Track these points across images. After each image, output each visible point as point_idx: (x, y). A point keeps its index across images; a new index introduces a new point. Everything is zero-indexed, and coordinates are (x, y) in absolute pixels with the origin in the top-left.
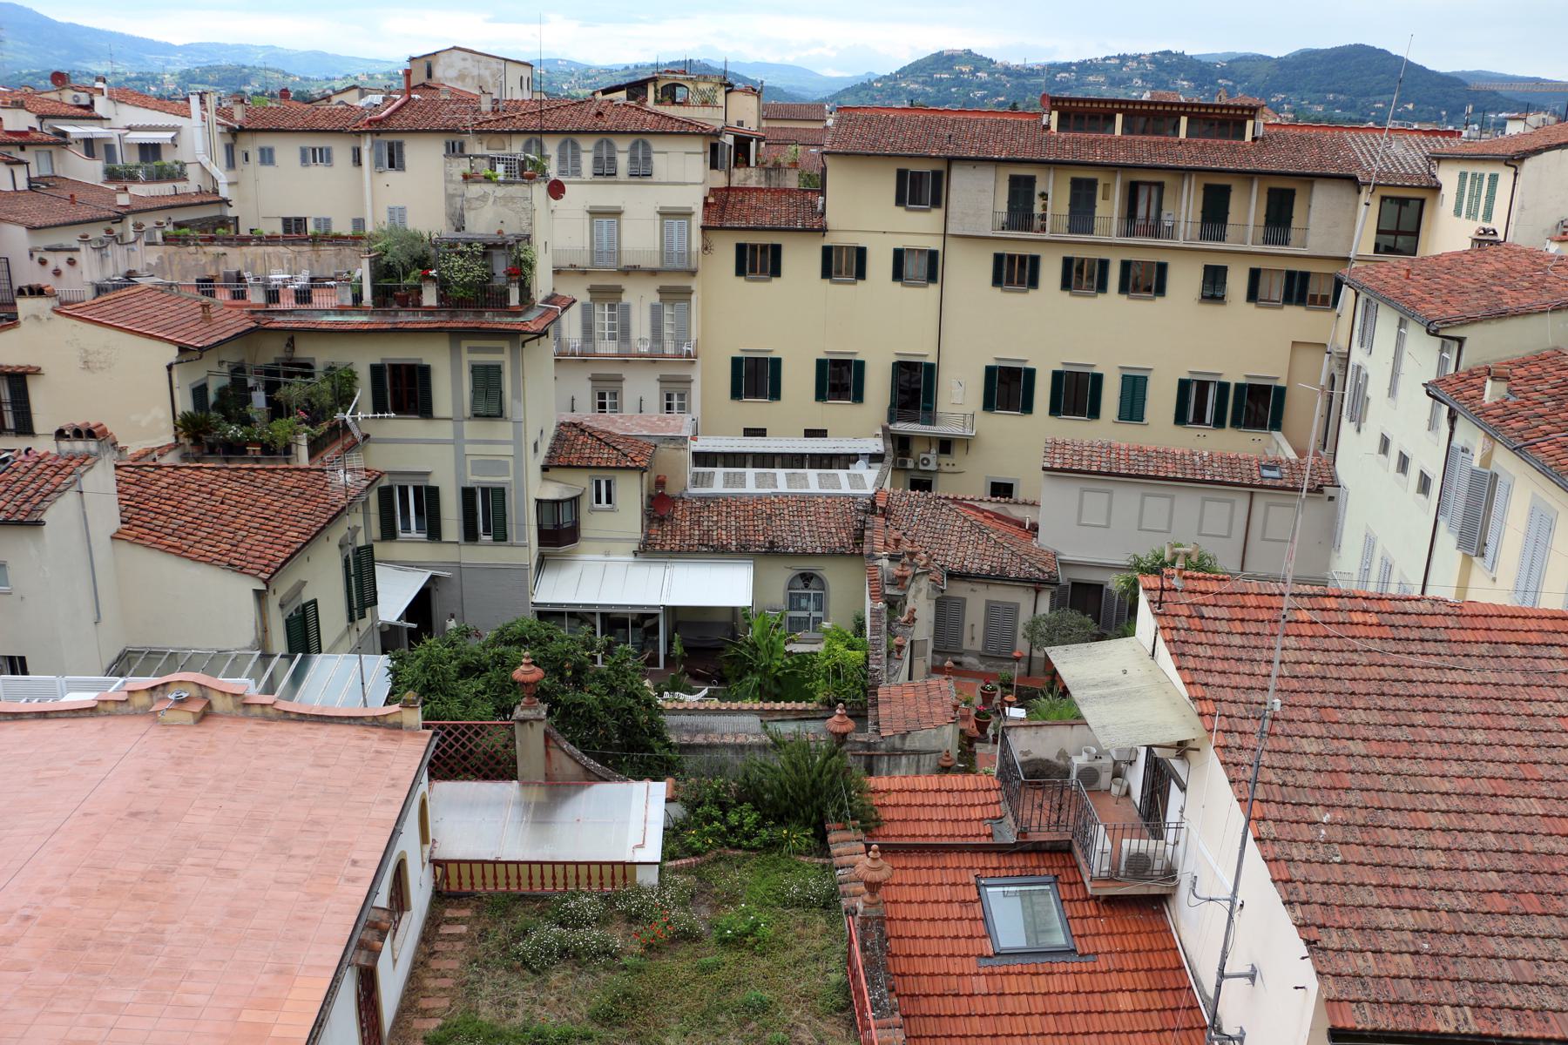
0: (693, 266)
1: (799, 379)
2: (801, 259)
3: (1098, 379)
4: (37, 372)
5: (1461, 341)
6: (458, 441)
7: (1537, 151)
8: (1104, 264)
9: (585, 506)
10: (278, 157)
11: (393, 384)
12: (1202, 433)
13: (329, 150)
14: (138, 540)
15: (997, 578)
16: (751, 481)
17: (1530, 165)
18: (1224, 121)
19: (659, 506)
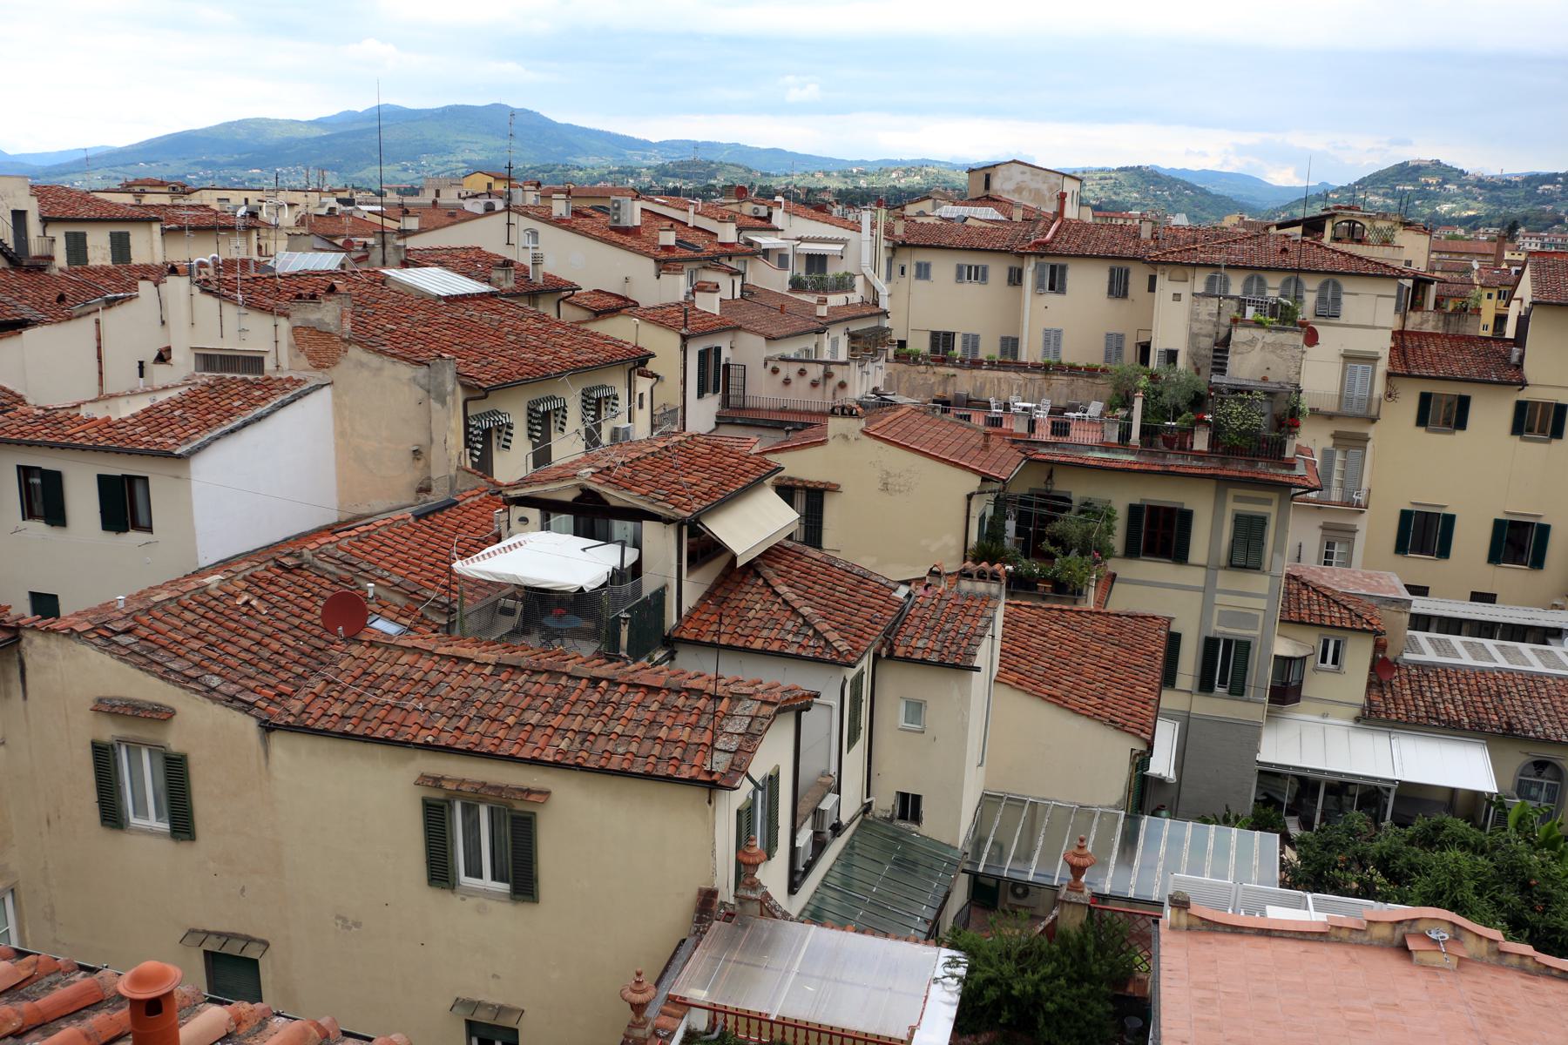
0: (1374, 412)
1: (1472, 539)
2: (1491, 414)
4: (834, 488)
6: (1208, 590)
9: (1309, 664)
10: (933, 271)
11: (1148, 525)
13: (985, 269)
14: (1018, 686)
16: (1462, 652)
19: (1382, 669)
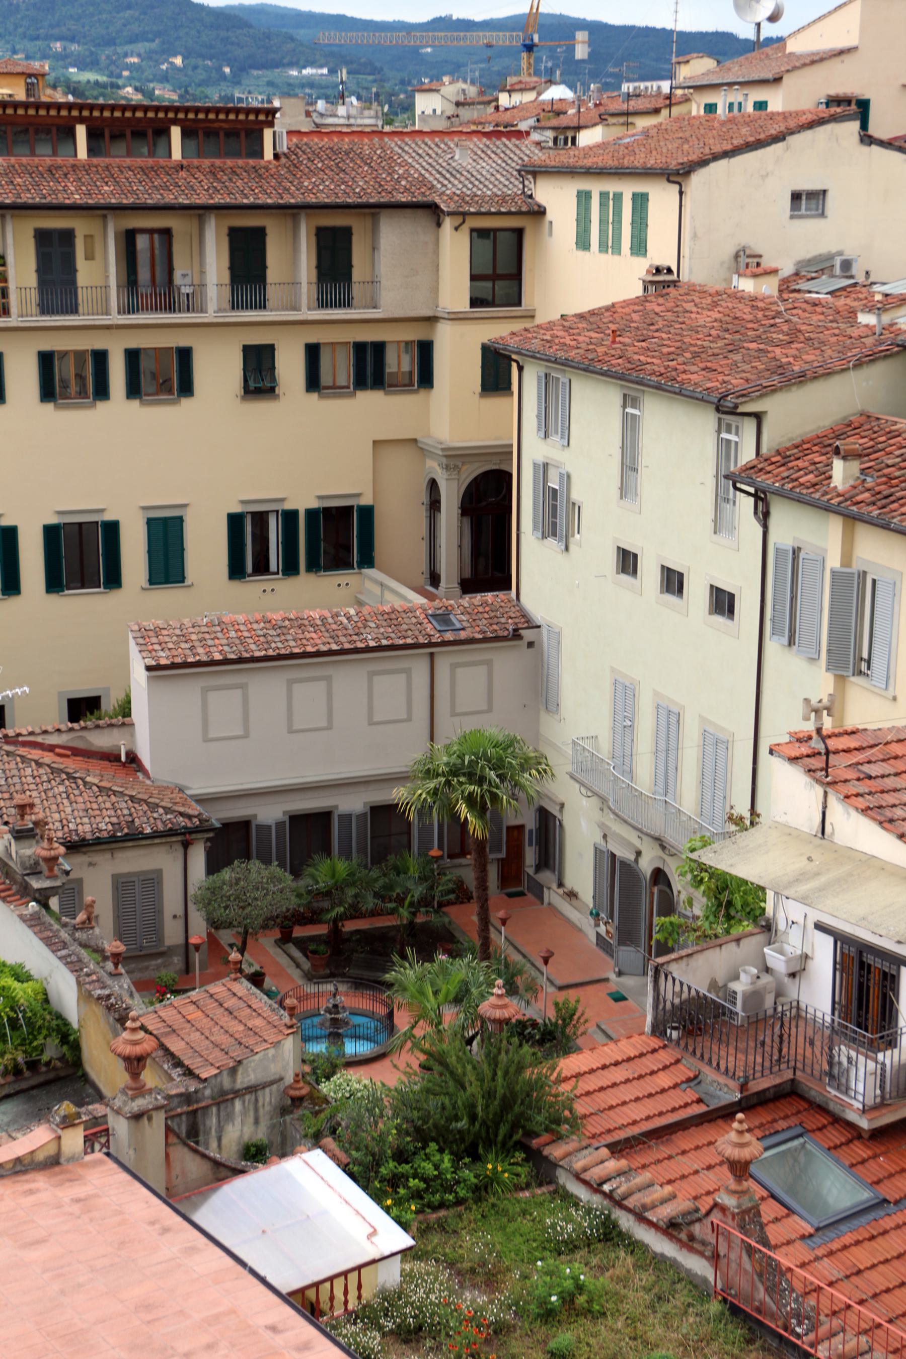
3: (112, 529)
5: (758, 417)
7: (703, 163)
8: (100, 358)
12: (268, 586)
15: (127, 838)
17: (698, 179)
18: (231, 132)
